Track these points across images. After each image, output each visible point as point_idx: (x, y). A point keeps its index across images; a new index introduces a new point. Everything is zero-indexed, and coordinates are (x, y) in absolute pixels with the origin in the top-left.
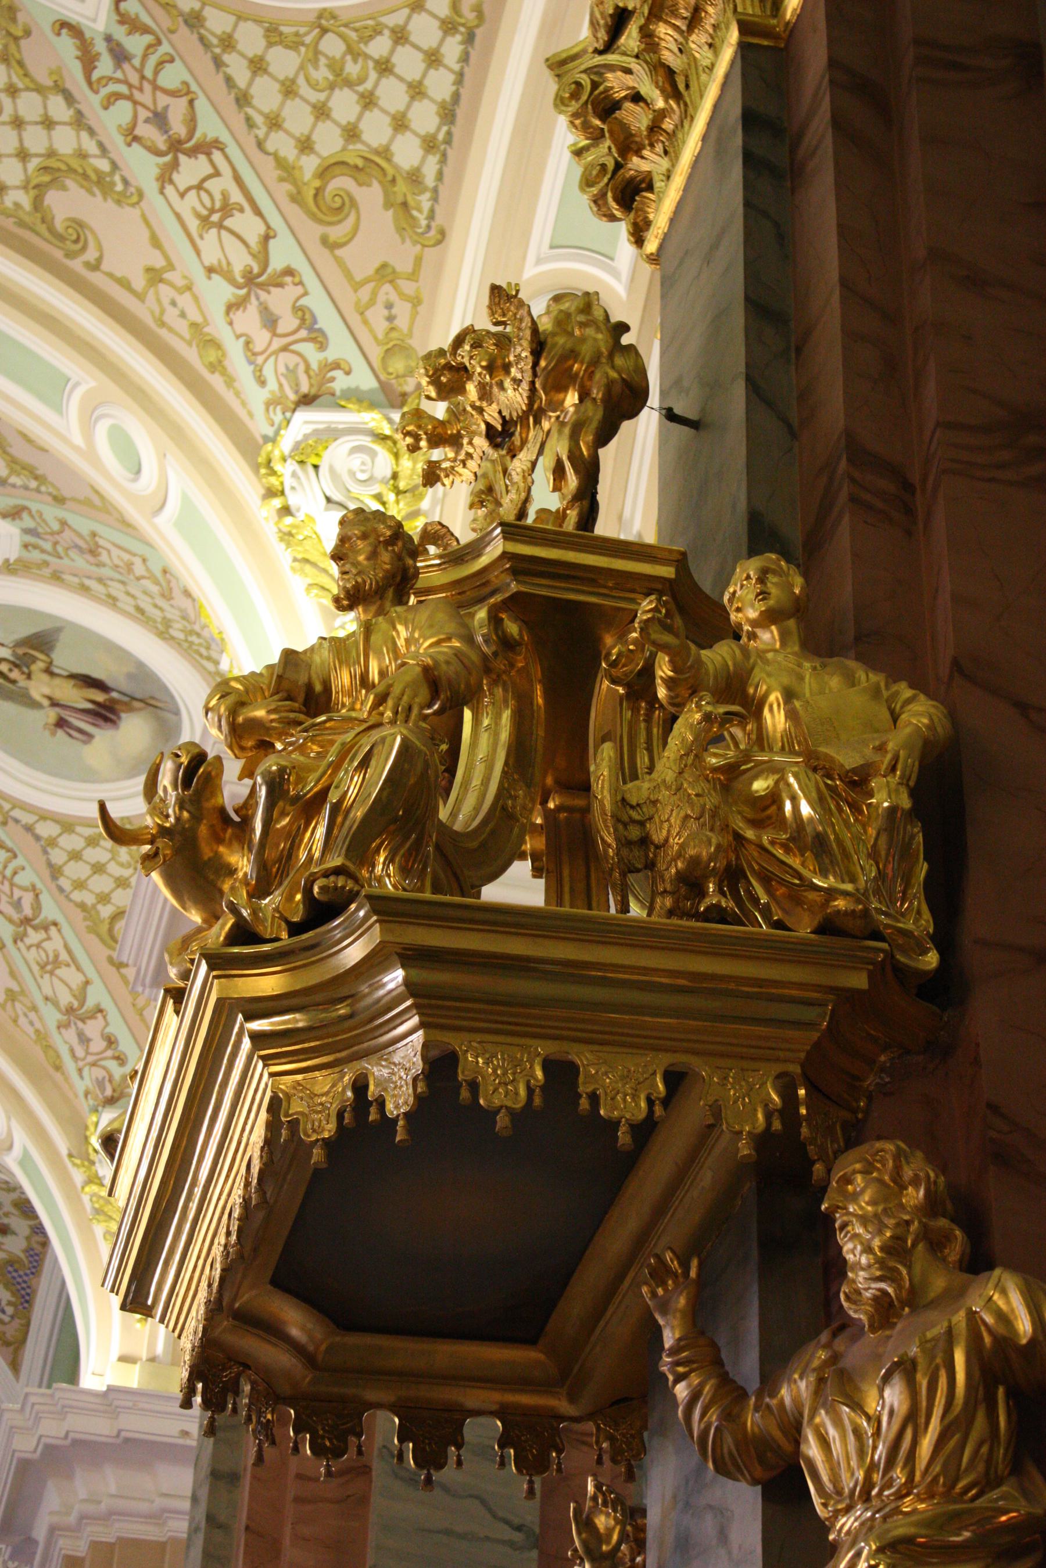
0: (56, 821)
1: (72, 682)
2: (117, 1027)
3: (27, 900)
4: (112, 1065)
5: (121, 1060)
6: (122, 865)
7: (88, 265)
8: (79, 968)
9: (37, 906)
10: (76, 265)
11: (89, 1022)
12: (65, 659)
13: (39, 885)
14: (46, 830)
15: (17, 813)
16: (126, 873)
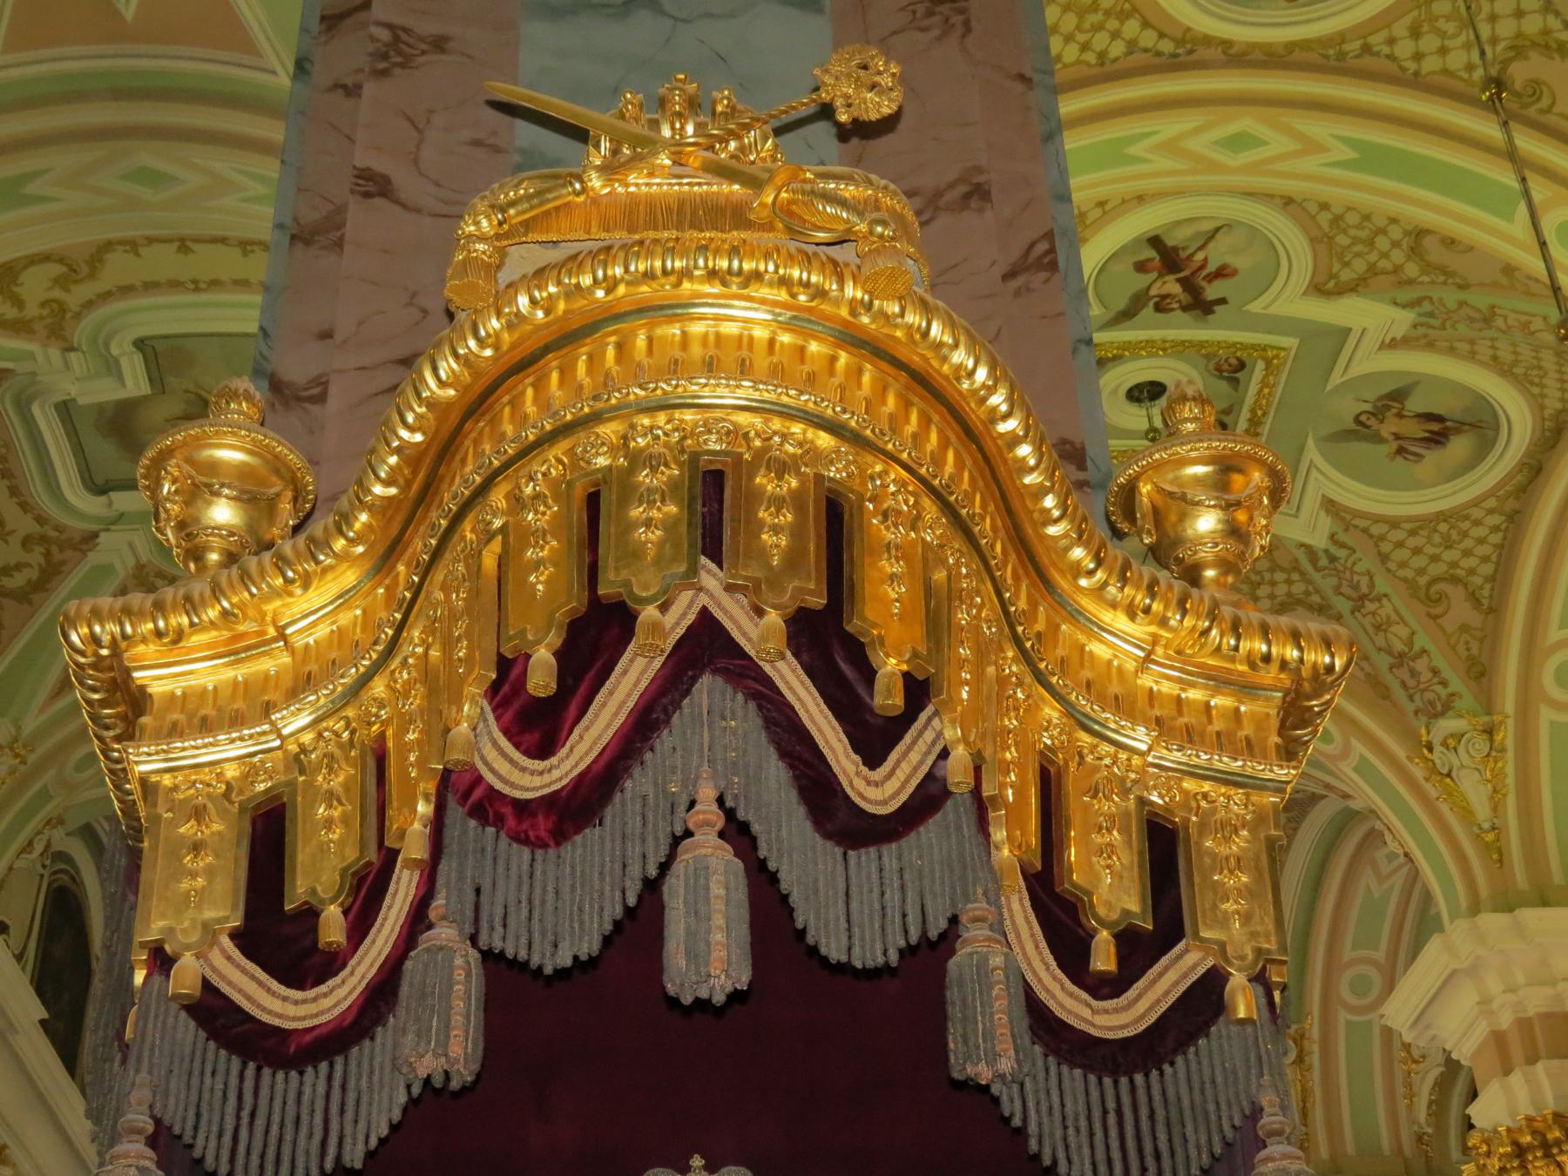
0: (1387, 523)
1: (1415, 420)
2: (1440, 662)
3: (1364, 582)
4: (1439, 688)
5: (1444, 684)
6: (1434, 546)
7: (1542, 112)
8: (1406, 624)
9: (1372, 585)
10: (1532, 112)
11: (1418, 661)
12: (1415, 404)
13: (1373, 570)
14: (1377, 530)
15: (1357, 522)
16: (1438, 551)
